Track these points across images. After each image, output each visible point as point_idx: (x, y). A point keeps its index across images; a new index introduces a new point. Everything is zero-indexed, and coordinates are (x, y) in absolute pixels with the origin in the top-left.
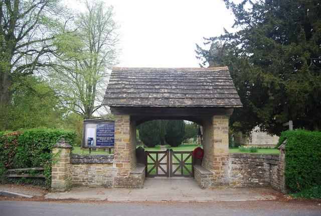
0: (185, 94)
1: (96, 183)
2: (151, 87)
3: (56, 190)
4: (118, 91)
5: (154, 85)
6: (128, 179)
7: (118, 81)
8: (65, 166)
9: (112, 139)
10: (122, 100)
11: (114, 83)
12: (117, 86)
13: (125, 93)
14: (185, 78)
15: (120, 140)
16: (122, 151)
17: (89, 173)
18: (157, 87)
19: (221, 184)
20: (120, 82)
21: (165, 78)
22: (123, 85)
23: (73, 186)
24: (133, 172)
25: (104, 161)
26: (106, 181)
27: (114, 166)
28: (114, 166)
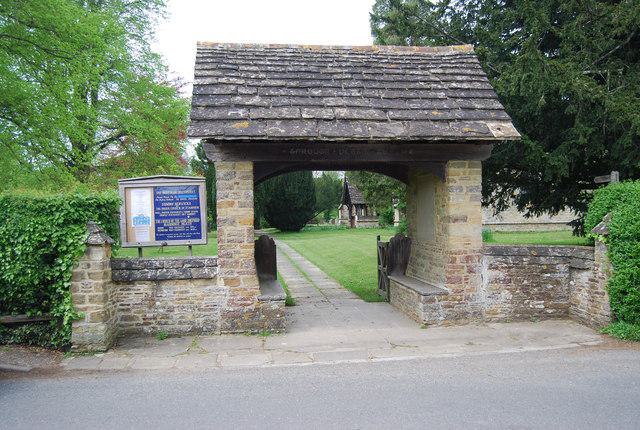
0: (386, 110)
1: (178, 326)
2: (301, 92)
3: (84, 350)
4: (223, 101)
5: (306, 88)
6: (254, 313)
7: (218, 77)
8: (105, 289)
9: (193, 224)
10: (236, 125)
11: (208, 81)
12: (216, 91)
13: (242, 106)
14: (377, 71)
15: (233, 223)
16: (238, 248)
17: (158, 303)
18: (316, 92)
19: (465, 314)
20: (224, 80)
21: (329, 70)
22: (233, 88)
23: (123, 336)
24: (265, 297)
25: (196, 271)
26: (201, 320)
27: (220, 283)
28: (220, 283)
